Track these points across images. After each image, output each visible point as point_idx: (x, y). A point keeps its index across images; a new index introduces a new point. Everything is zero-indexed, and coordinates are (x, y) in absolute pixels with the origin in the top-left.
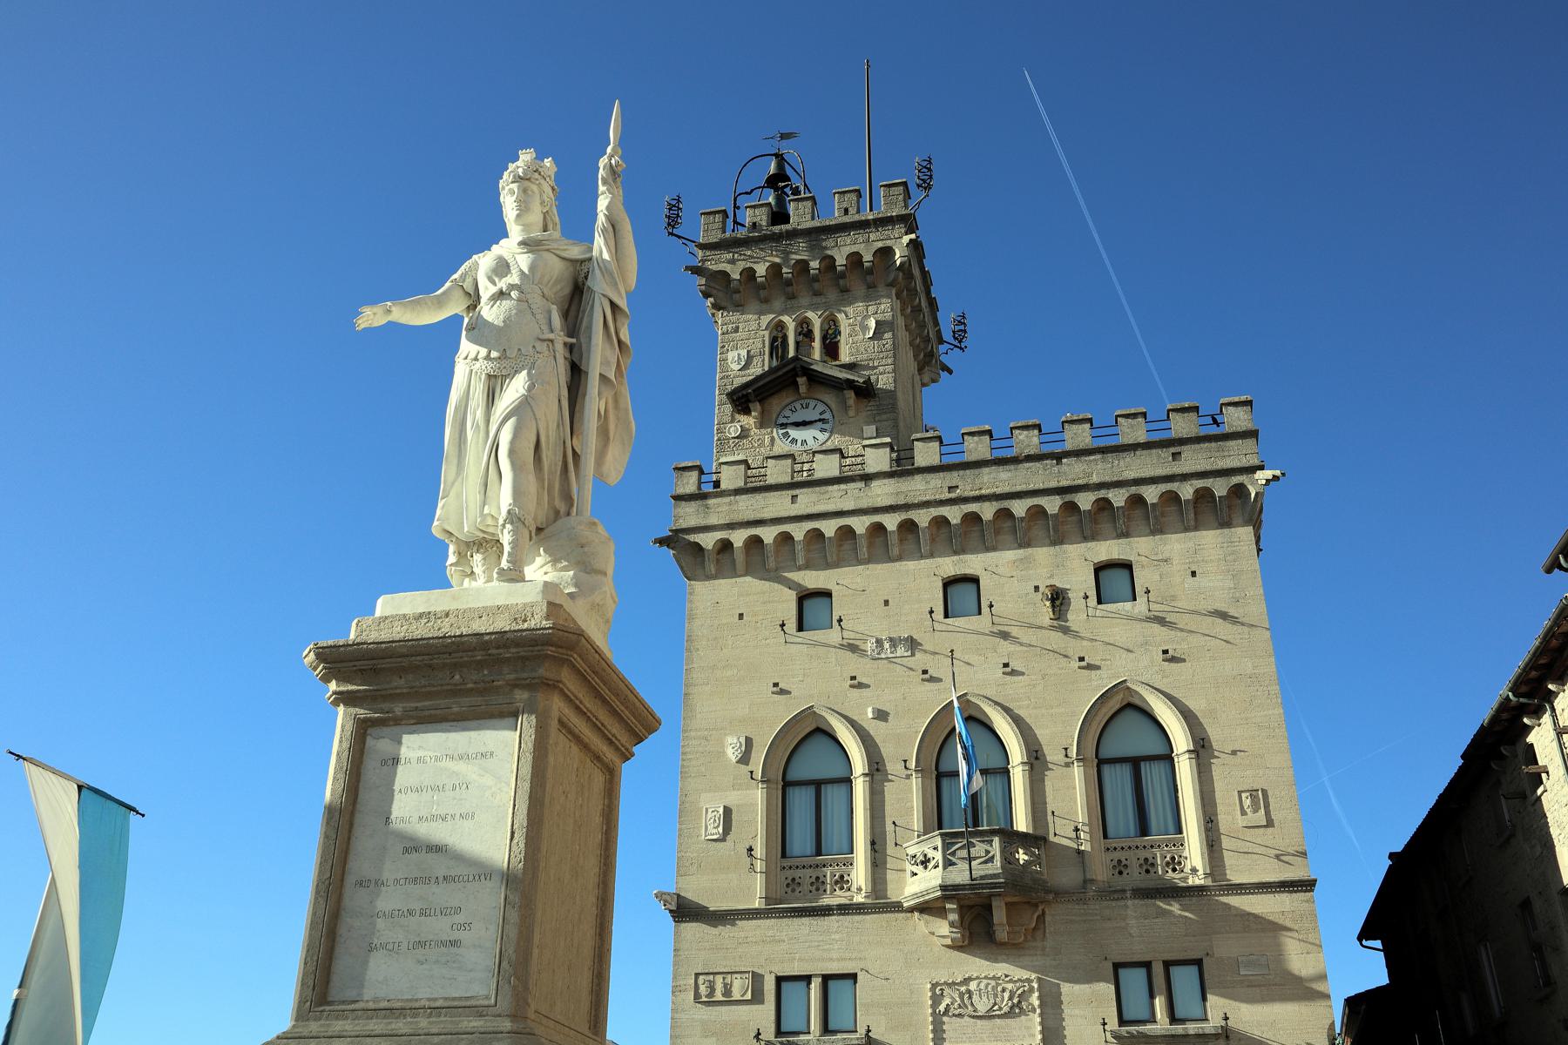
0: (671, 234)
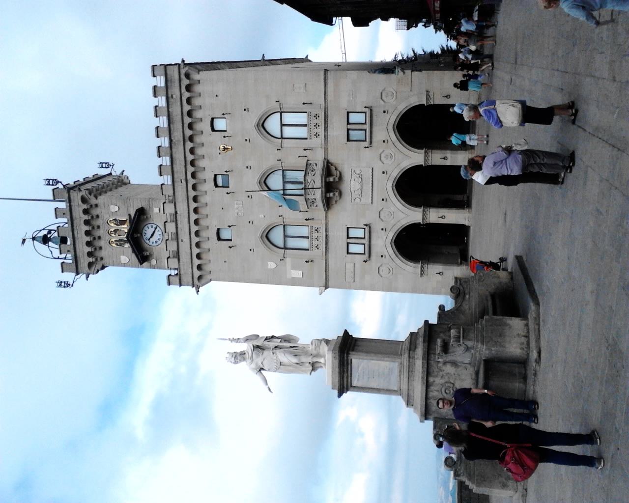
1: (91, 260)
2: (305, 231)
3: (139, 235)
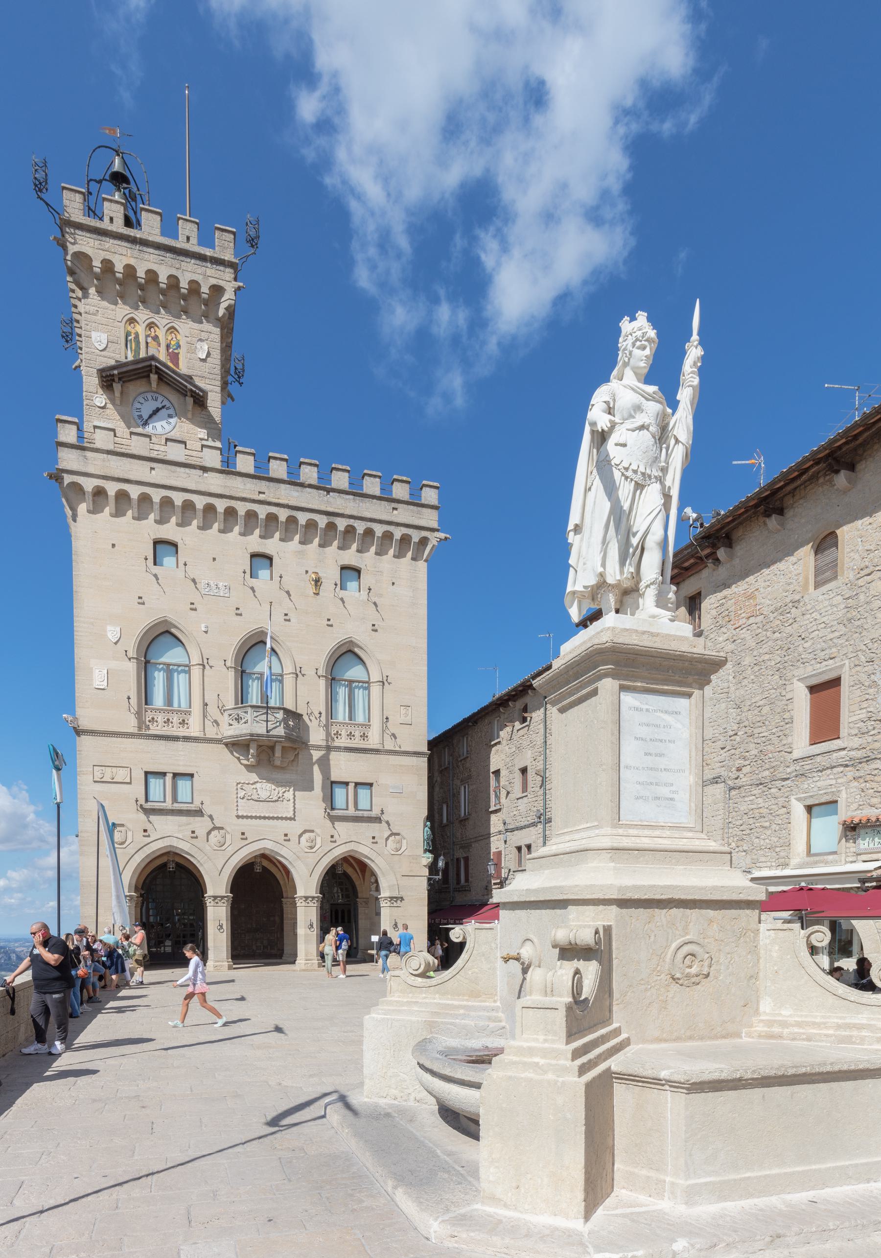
2: (180, 699)
3: (154, 384)
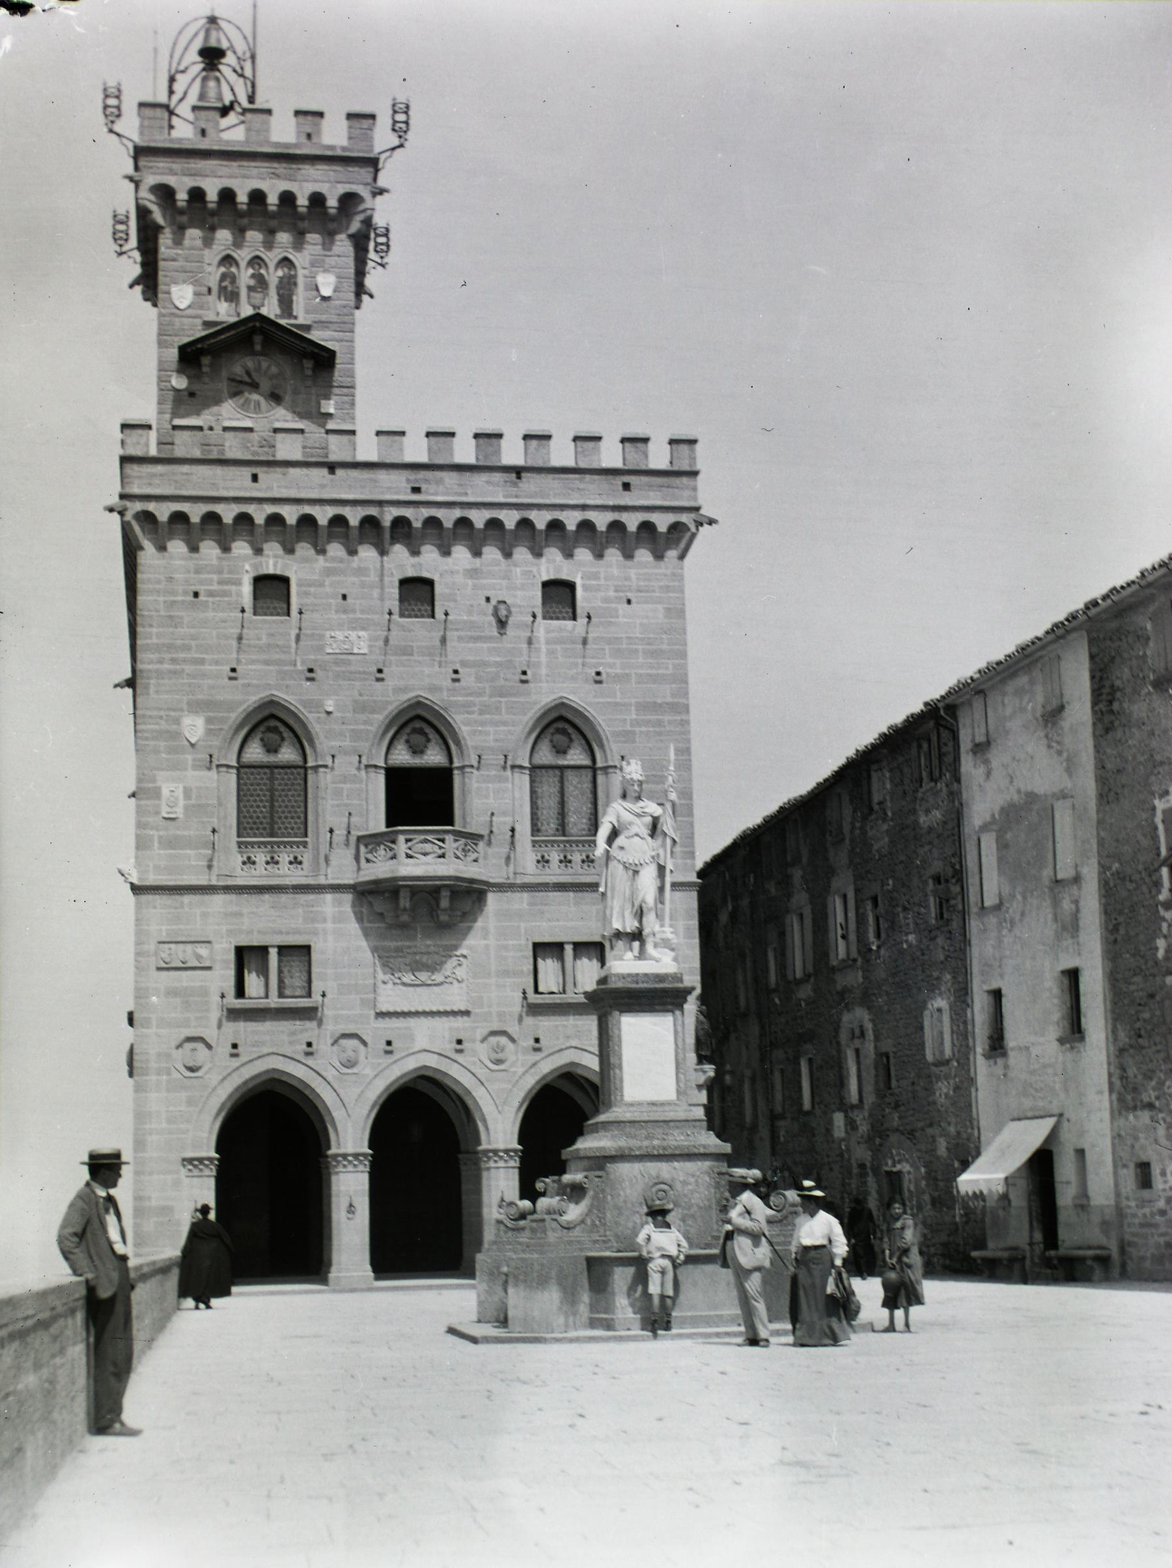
0: (111, 131)
1: (182, 196)
3: (258, 348)
